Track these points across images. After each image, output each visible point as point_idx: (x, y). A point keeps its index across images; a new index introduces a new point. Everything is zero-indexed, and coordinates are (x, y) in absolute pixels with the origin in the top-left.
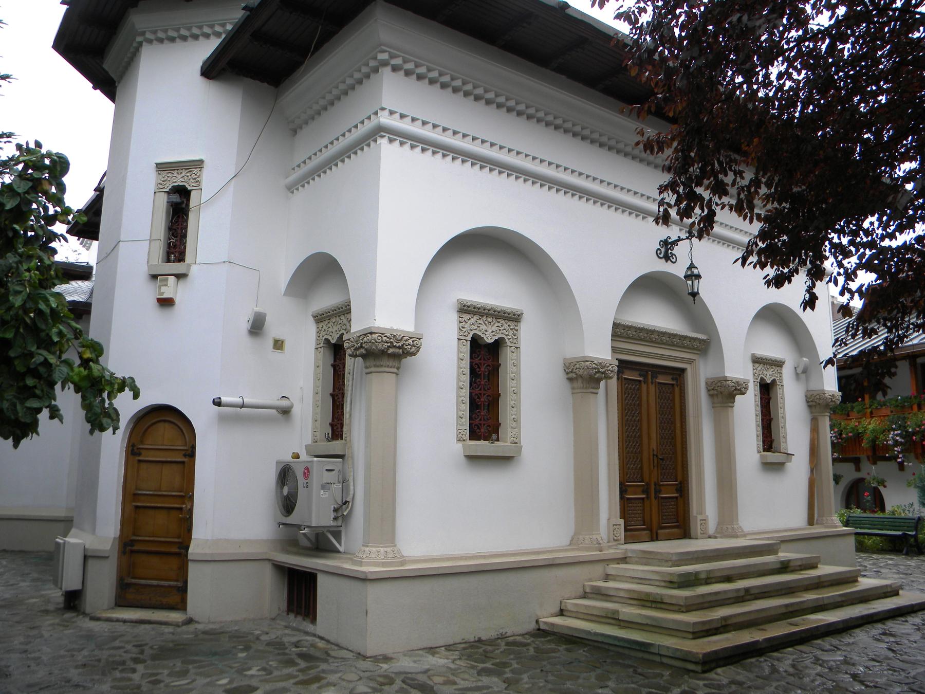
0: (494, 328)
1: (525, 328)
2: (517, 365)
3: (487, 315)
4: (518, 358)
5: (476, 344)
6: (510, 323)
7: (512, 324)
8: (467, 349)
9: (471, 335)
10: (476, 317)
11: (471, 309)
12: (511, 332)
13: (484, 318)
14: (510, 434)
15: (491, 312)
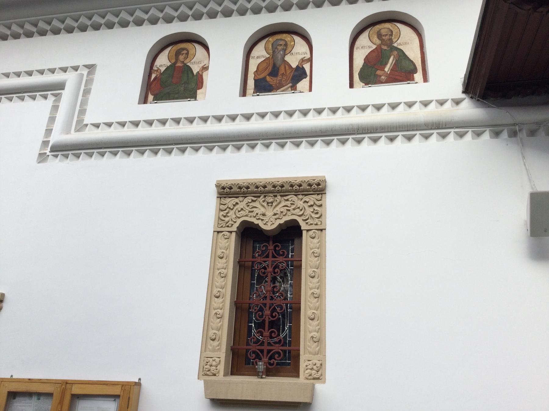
0: (278, 209)
1: (332, 202)
2: (320, 256)
3: (266, 193)
4: (322, 246)
5: (249, 233)
6: (306, 198)
7: (312, 199)
8: (230, 245)
9: (237, 224)
10: (249, 199)
11: (235, 189)
12: (309, 211)
13: (261, 199)
14: (303, 365)
15: (269, 188)
